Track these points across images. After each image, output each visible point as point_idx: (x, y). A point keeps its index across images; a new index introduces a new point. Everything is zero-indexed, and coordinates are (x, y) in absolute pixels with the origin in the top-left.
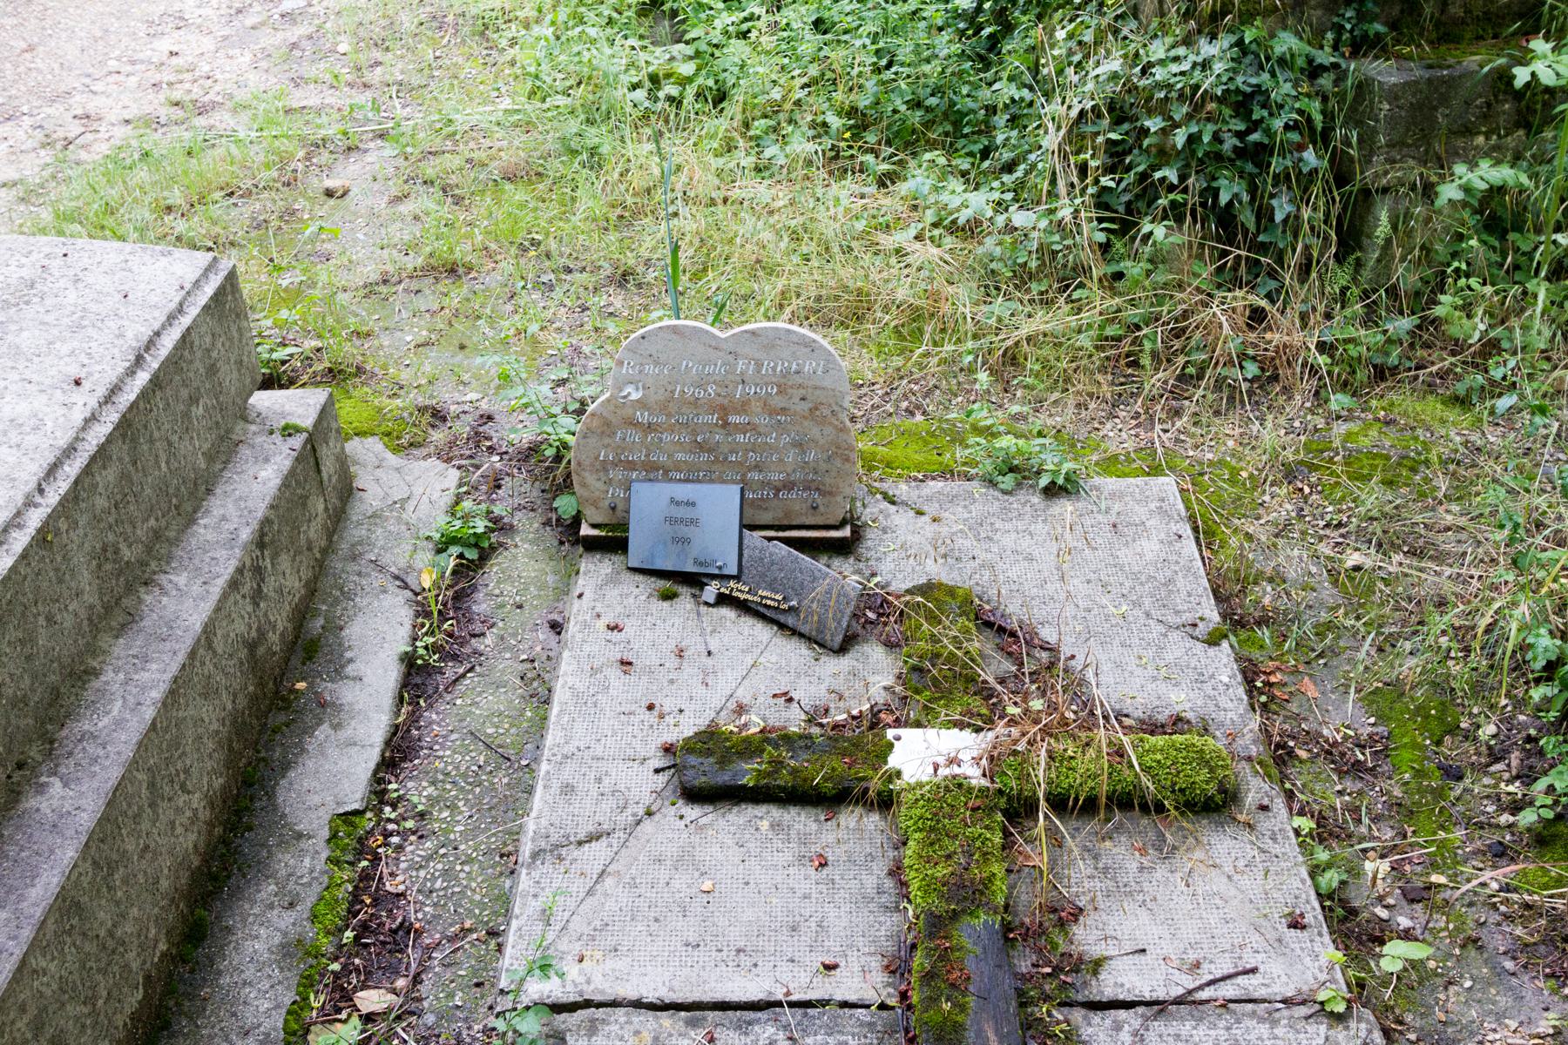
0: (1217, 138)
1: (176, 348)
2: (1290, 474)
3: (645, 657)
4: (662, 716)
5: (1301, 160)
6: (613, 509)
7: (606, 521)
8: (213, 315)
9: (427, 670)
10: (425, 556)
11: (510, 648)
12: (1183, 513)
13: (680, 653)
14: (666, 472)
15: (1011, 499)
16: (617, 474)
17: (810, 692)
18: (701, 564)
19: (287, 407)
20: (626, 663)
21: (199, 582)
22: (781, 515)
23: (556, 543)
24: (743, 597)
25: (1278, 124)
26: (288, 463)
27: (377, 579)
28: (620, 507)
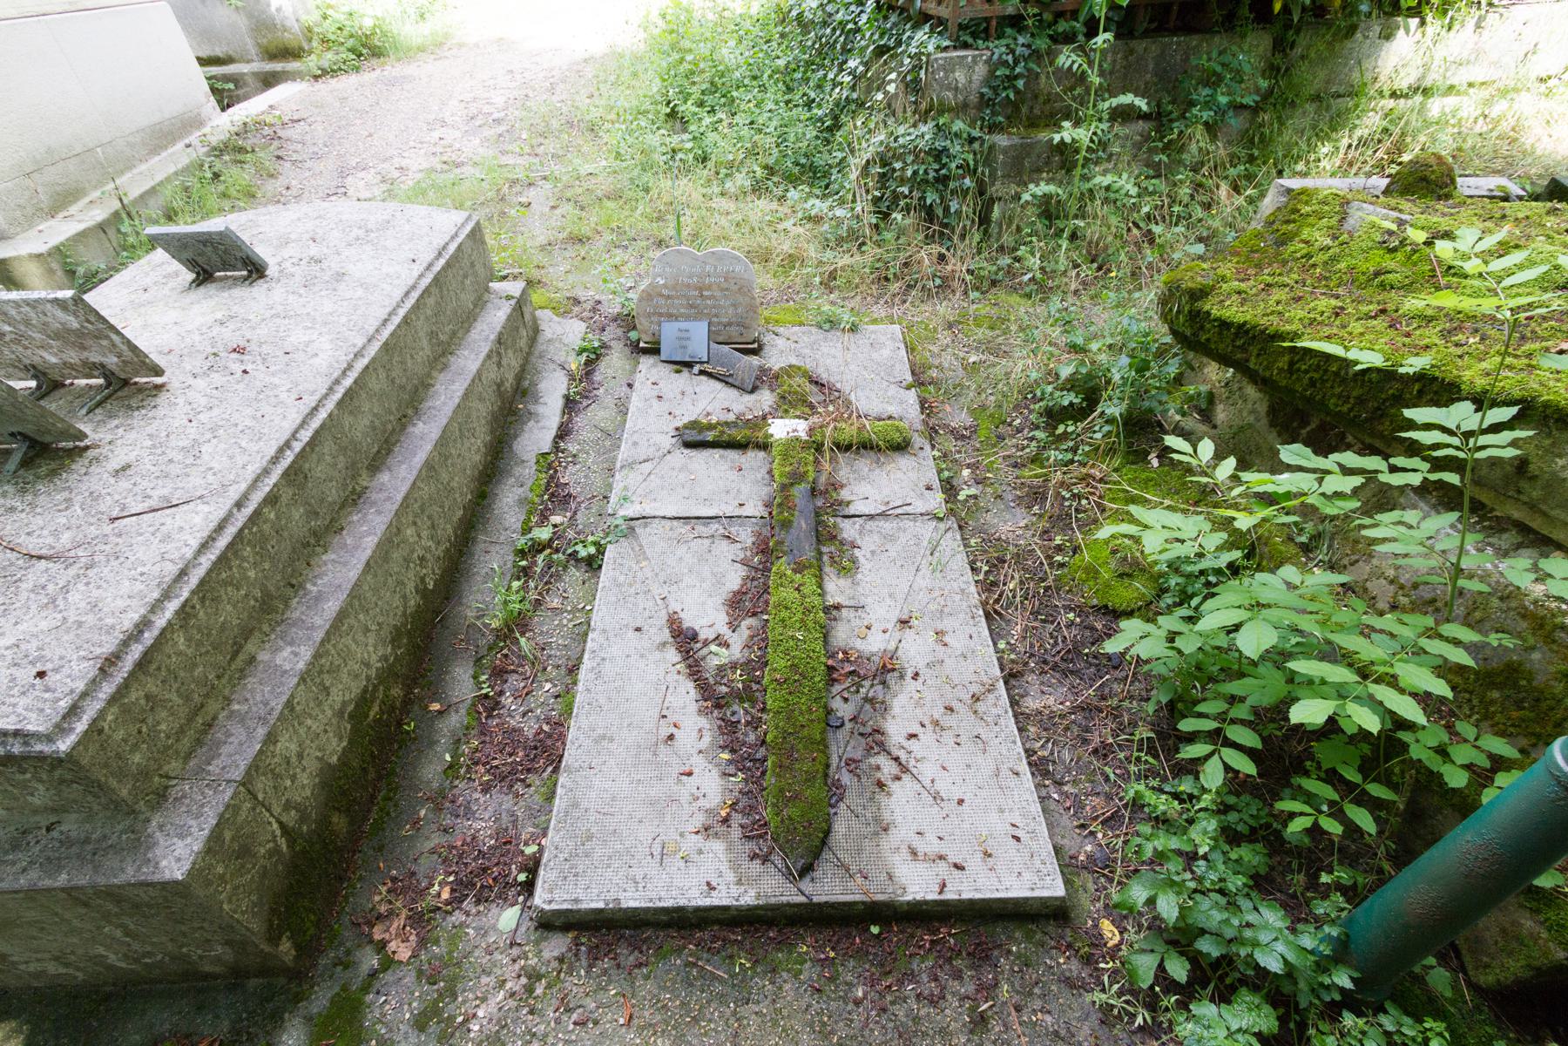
0: (926, 172)
2: (950, 326)
9: (574, 401)
27: (552, 366)
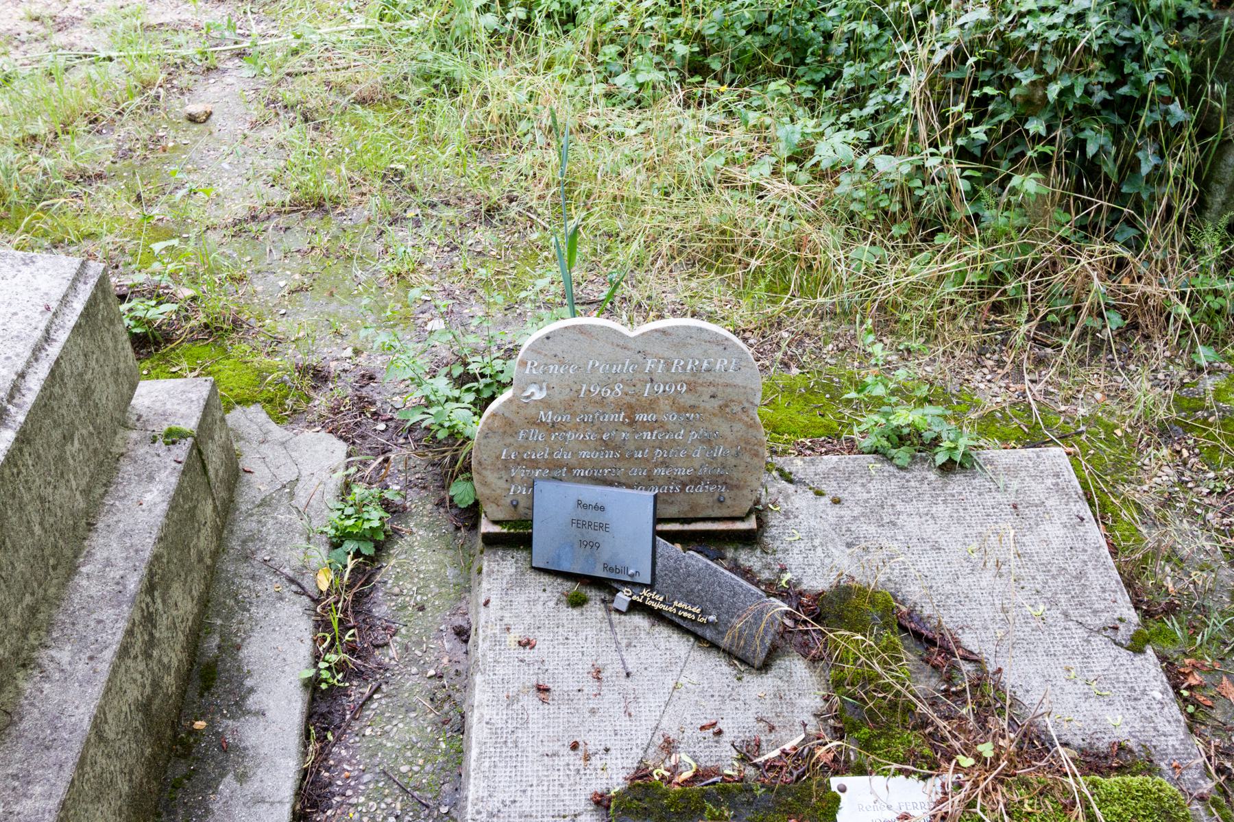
0: (1088, 93)
1: (44, 389)
2: (1165, 432)
3: (563, 683)
4: (587, 758)
5: (1167, 112)
6: (515, 507)
7: (507, 517)
8: (84, 334)
9: (334, 693)
10: (320, 554)
11: (415, 661)
12: (1081, 492)
13: (597, 675)
14: (570, 470)
15: (908, 476)
16: (519, 473)
17: (738, 723)
18: (611, 570)
19: (169, 406)
20: (542, 690)
21: (84, 657)
22: (687, 508)
23: (452, 529)
24: (656, 606)
25: (1148, 77)
26: (174, 480)
27: (272, 585)
28: (522, 503)
